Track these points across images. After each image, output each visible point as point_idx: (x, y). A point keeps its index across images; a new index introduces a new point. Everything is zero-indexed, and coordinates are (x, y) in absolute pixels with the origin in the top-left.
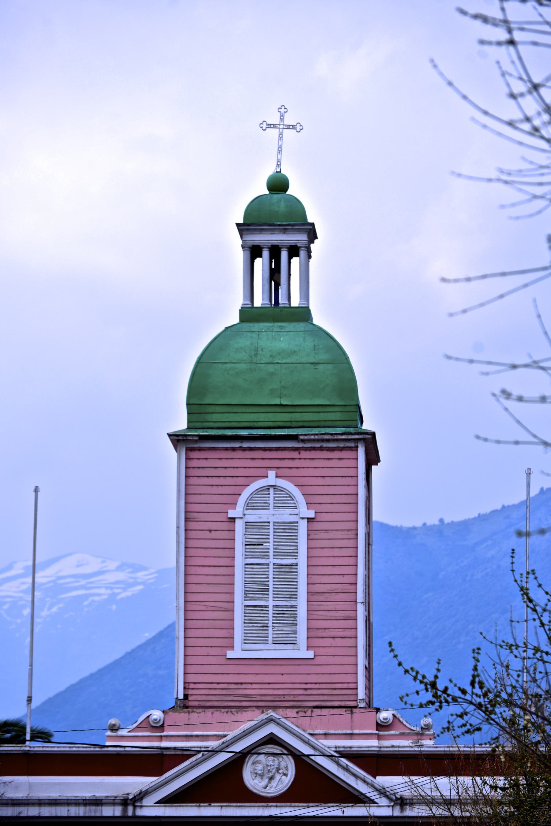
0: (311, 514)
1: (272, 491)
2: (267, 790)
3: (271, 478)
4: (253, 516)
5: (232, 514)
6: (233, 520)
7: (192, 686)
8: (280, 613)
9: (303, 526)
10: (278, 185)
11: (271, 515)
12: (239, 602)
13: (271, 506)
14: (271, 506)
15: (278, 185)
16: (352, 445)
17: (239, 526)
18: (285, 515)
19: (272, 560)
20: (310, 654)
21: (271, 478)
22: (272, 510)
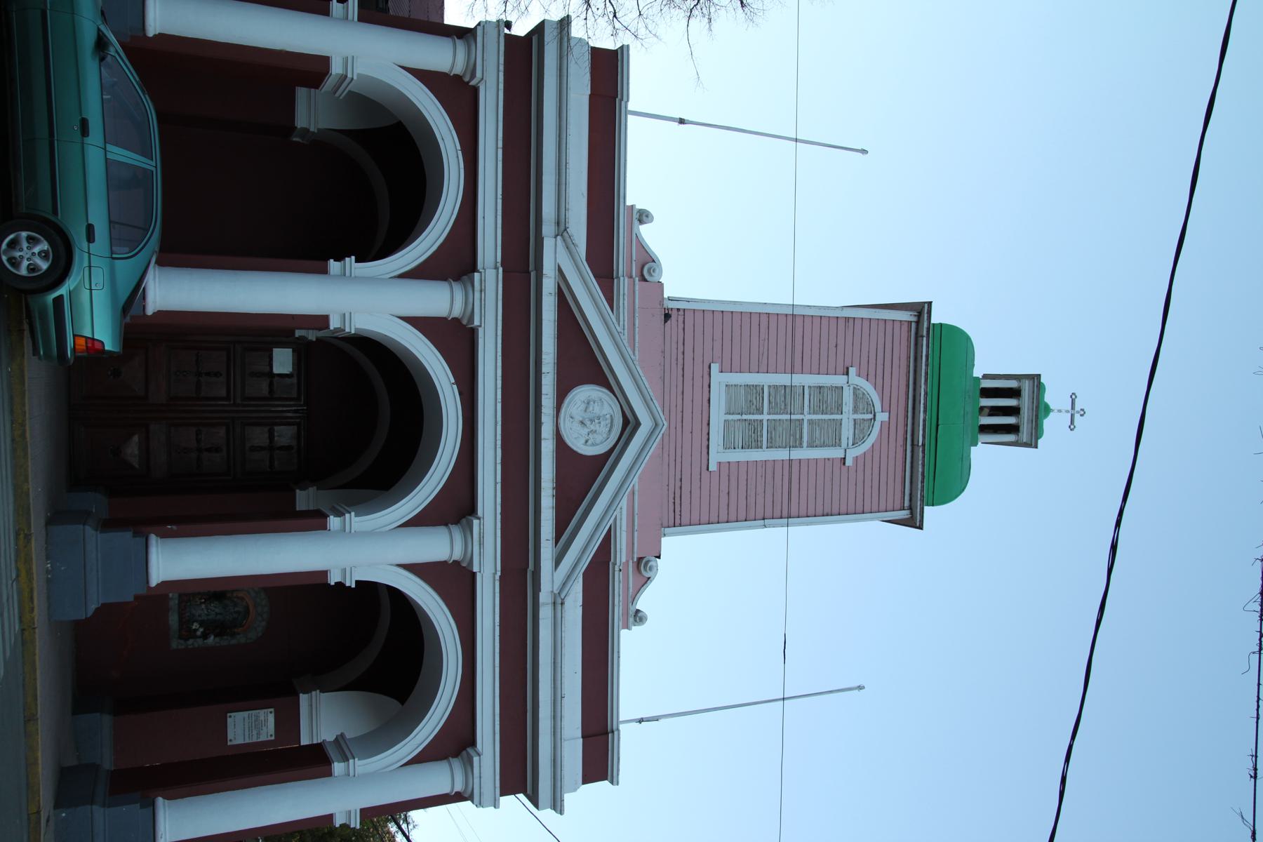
0: (849, 462)
1: (871, 416)
2: (568, 418)
3: (882, 417)
4: (848, 397)
5: (852, 371)
6: (847, 374)
7: (681, 319)
8: (755, 427)
9: (836, 453)
10: (1012, 410)
11: (847, 418)
12: (800, 380)
13: (856, 416)
14: (856, 416)
15: (1012, 410)
16: (907, 504)
17: (839, 380)
18: (847, 432)
19: (807, 417)
20: (713, 467)
21: (882, 417)
22: (844, 417)
